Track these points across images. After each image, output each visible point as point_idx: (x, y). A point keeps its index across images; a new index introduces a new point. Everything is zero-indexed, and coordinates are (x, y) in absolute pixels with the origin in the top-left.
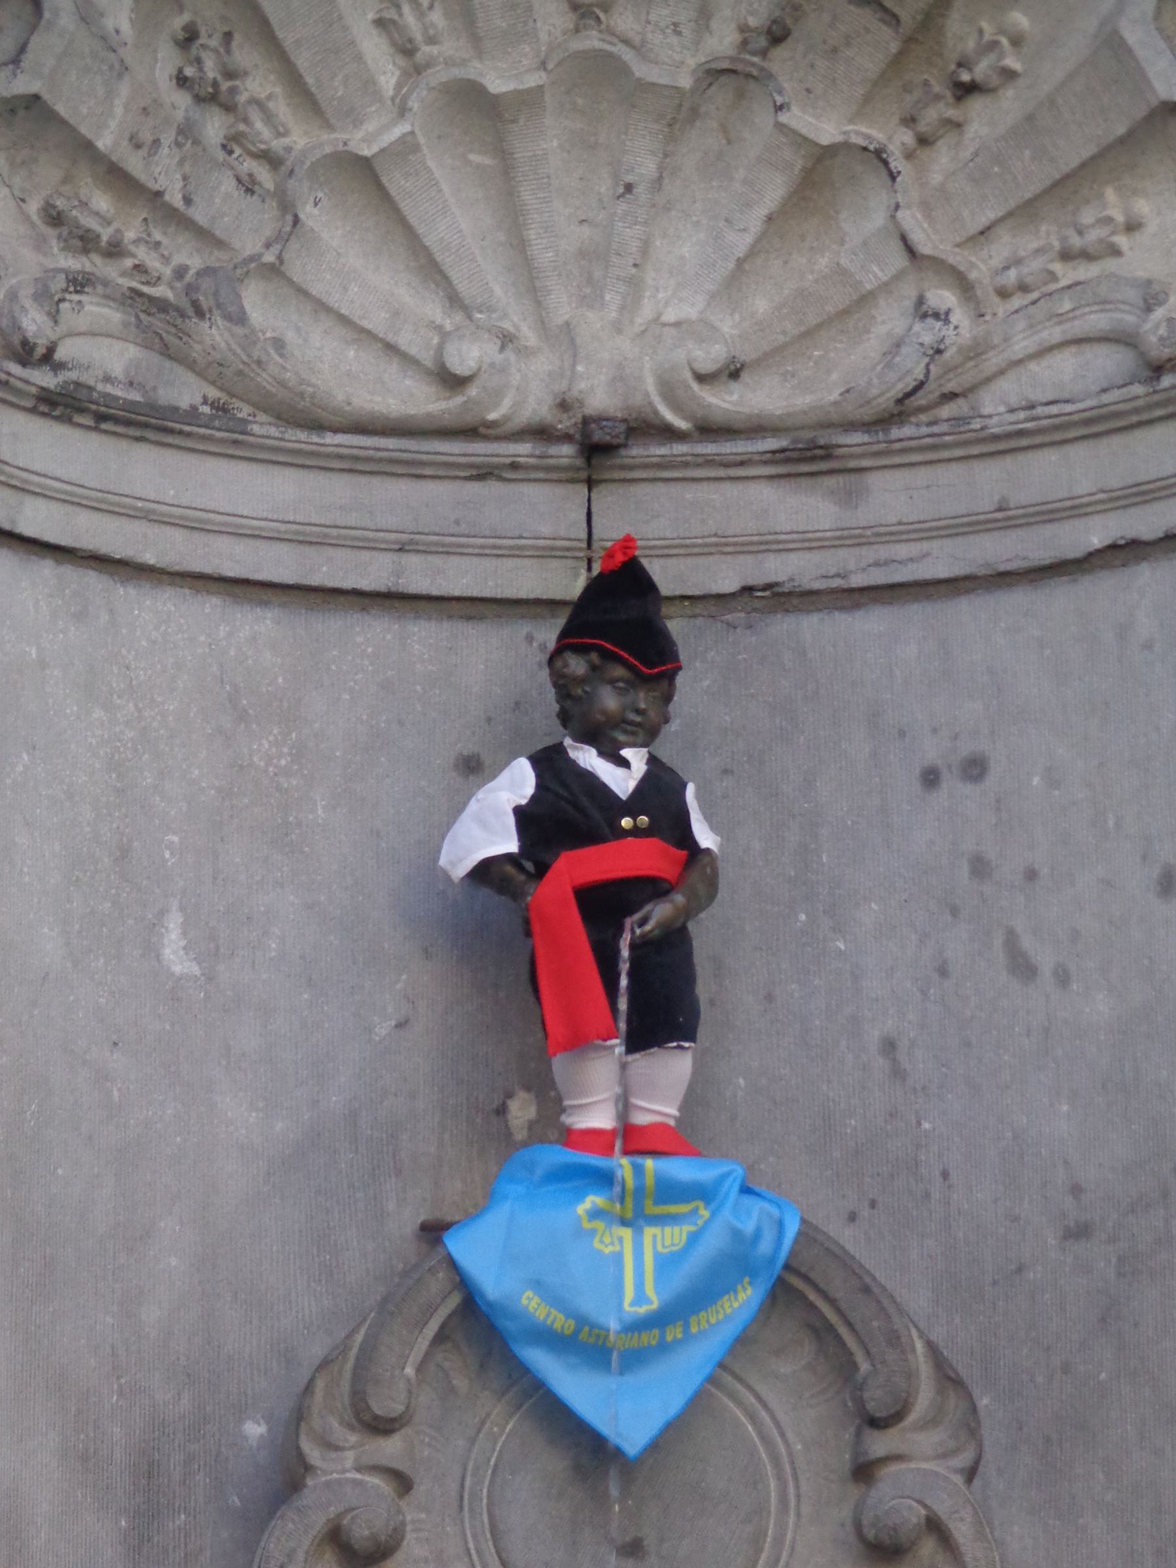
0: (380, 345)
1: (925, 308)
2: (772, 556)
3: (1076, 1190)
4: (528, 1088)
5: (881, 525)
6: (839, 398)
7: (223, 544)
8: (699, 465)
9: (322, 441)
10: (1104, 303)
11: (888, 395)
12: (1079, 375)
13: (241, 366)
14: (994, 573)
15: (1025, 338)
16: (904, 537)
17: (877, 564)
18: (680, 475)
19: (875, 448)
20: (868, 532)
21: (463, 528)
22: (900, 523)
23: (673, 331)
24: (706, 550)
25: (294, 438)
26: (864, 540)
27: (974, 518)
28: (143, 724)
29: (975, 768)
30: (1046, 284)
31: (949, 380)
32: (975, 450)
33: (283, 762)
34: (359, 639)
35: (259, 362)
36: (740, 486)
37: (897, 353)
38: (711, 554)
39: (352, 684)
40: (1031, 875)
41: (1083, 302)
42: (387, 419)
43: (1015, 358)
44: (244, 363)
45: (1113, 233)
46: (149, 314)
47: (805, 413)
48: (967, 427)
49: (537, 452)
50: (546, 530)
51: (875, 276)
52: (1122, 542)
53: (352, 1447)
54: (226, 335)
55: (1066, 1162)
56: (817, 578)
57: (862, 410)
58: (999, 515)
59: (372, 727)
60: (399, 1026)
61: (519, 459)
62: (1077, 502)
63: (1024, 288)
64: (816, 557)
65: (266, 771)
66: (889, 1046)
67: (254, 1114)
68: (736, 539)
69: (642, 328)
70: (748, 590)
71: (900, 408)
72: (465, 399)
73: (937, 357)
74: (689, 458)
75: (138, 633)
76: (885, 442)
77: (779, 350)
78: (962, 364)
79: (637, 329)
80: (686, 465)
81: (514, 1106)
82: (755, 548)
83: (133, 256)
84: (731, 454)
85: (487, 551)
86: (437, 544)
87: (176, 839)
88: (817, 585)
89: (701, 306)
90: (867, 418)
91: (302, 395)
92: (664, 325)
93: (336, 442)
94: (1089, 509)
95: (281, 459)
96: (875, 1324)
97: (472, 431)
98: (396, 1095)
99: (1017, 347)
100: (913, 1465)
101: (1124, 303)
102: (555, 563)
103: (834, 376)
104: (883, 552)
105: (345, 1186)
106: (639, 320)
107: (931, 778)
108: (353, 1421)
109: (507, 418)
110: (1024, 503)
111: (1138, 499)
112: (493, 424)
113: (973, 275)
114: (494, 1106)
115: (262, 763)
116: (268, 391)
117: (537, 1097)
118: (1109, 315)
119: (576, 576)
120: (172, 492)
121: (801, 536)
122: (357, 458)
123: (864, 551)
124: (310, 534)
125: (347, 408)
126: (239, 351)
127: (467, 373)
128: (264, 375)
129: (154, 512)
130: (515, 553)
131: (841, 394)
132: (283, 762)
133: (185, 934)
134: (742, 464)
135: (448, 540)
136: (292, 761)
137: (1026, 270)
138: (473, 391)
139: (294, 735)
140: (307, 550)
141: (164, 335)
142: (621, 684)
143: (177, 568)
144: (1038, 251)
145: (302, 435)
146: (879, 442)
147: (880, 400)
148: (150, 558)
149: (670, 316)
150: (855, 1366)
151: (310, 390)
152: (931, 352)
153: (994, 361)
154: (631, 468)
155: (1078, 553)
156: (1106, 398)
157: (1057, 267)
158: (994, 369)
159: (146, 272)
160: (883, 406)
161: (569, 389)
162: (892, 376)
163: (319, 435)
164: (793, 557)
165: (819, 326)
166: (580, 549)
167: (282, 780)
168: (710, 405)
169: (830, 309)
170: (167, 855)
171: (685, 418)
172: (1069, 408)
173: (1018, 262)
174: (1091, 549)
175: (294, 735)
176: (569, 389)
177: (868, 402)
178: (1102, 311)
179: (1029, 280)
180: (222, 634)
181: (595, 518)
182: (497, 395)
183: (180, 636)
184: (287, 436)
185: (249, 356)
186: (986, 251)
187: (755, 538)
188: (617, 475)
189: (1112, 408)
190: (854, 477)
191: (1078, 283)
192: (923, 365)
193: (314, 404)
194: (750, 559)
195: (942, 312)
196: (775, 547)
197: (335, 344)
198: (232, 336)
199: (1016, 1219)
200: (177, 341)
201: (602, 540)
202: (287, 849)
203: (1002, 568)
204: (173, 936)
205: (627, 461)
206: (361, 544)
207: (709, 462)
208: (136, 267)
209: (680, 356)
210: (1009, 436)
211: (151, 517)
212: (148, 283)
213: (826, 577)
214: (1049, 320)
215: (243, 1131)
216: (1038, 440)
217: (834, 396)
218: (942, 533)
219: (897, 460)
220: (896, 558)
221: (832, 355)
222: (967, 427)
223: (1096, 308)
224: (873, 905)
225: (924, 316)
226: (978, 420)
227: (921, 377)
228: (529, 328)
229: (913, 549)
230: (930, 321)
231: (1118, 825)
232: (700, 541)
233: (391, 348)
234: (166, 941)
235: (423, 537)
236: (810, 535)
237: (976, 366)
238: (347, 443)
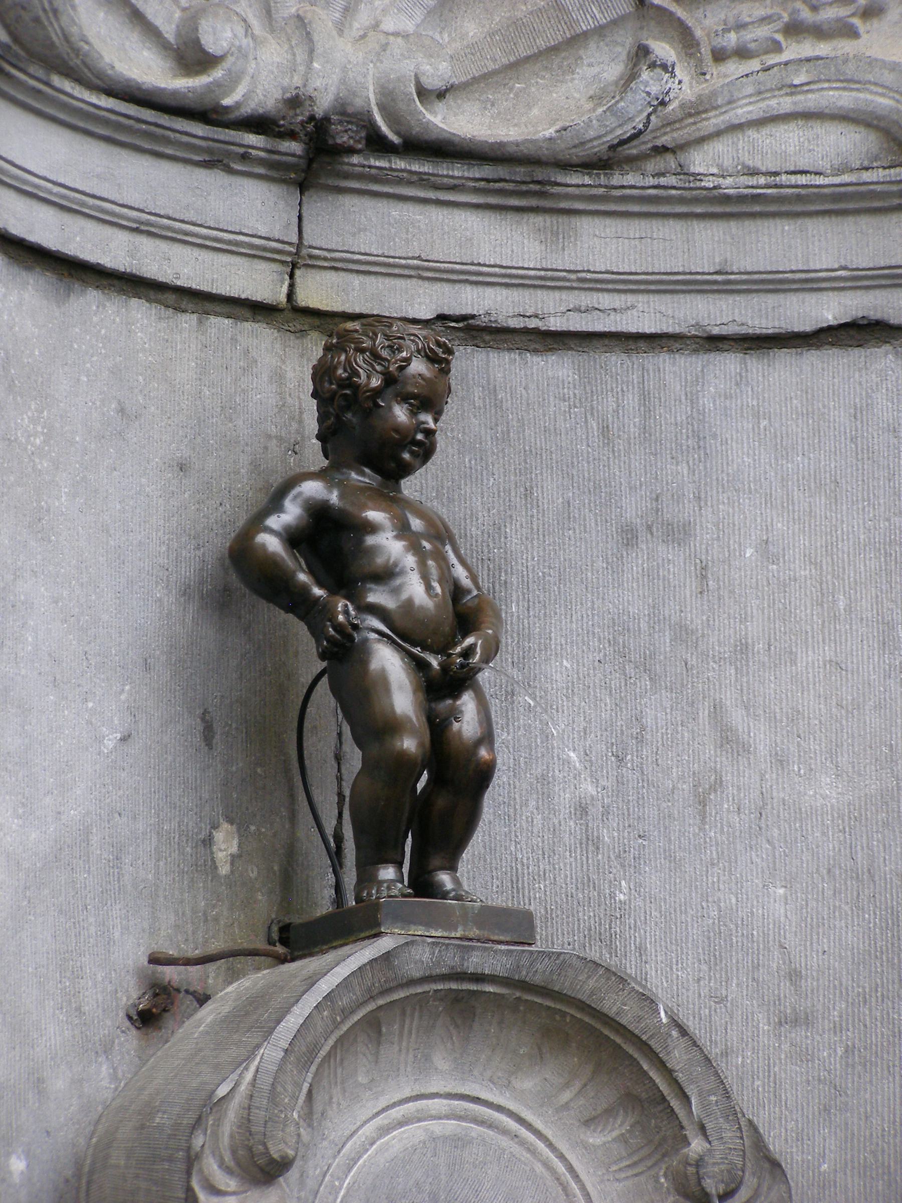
0: (128, 10)
1: (652, 57)
2: (469, 288)
3: (794, 976)
4: (231, 821)
5: (589, 271)
6: (554, 135)
8: (410, 183)
10: (849, 82)
11: (605, 139)
12: (825, 151)
13: (41, 13)
14: (705, 335)
15: (750, 103)
16: (610, 286)
17: (578, 310)
18: (391, 191)
19: (595, 191)
20: (573, 276)
21: (190, 216)
22: (607, 272)
23: (400, 40)
24: (406, 272)
25: (79, 96)
26: (568, 284)
27: (688, 277)
29: (678, 533)
30: (767, 52)
31: (665, 134)
32: (699, 210)
33: (38, 441)
34: (95, 319)
37: (622, 99)
38: (410, 277)
40: (743, 648)
41: (823, 77)
42: (139, 89)
43: (737, 122)
44: (44, 10)
45: (853, 15)
47: (517, 145)
48: (698, 184)
49: (269, 147)
51: (594, 17)
52: (865, 322)
53: (234, 1193)
55: (782, 947)
56: (514, 316)
57: (574, 150)
58: (719, 278)
59: (104, 414)
60: (124, 739)
61: (250, 151)
62: (813, 275)
63: (742, 53)
64: (515, 295)
65: (26, 449)
66: (582, 809)
67: (16, 821)
68: (438, 265)
69: (361, 33)
70: (442, 317)
71: (611, 154)
72: (211, 79)
73: (659, 108)
74: (405, 175)
76: (606, 187)
77: (485, 77)
78: (682, 119)
79: (355, 33)
80: (400, 181)
81: (219, 836)
82: (455, 277)
84: (447, 176)
85: (208, 243)
86: (169, 228)
88: (514, 323)
89: (419, 20)
90: (575, 160)
91: (77, 51)
92: (387, 34)
93: (109, 106)
94: (824, 285)
95: (62, 116)
96: (713, 1098)
97: (206, 113)
98: (120, 814)
99: (740, 111)
101: (876, 84)
102: (262, 265)
103: (535, 111)
105: (80, 908)
106: (356, 25)
107: (629, 537)
108: (232, 1164)
109: (238, 105)
110: (749, 269)
111: (889, 282)
112: (227, 109)
113: (698, 33)
114: (202, 836)
116: (53, 44)
117: (238, 830)
118: (854, 94)
119: (282, 282)
121: (503, 271)
122: (119, 127)
123: (564, 295)
125: (110, 72)
127: (219, 53)
128: (56, 26)
130: (230, 249)
131: (557, 131)
134: (453, 188)
135: (178, 225)
137: (748, 35)
138: (218, 73)
139: (45, 413)
140: (67, 218)
144: (765, 20)
146: (600, 186)
147: (595, 143)
149: (389, 25)
150: (686, 1142)
152: (656, 103)
153: (715, 121)
154: (347, 176)
155: (808, 328)
156: (866, 176)
157: (779, 37)
158: (712, 129)
160: (596, 150)
161: (305, 86)
162: (611, 122)
163: (98, 97)
164: (489, 291)
165: (527, 59)
166: (289, 254)
167: (37, 460)
168: (429, 122)
169: (542, 43)
171: (398, 133)
172: (820, 180)
173: (740, 26)
174: (825, 325)
176: (305, 86)
177: (583, 144)
178: (844, 89)
179: (752, 46)
181: (305, 222)
182: (234, 79)
186: (701, 10)
187: (458, 267)
188: (331, 182)
189: (872, 187)
190: (563, 219)
191: (818, 58)
192: (645, 114)
193: (84, 62)
194: (447, 288)
195: (669, 64)
196: (474, 278)
199: (722, 1000)
201: (311, 247)
202: (40, 535)
203: (716, 331)
205: (346, 168)
207: (422, 180)
209: (407, 68)
210: (741, 199)
213: (524, 316)
214: (780, 89)
216: (773, 208)
217: (550, 132)
218: (653, 287)
219: (613, 207)
220: (596, 306)
221: (533, 89)
222: (698, 184)
223: (838, 85)
224: (565, 663)
225: (652, 66)
226: (711, 178)
227: (641, 126)
228: (255, 16)
229: (617, 300)
230: (658, 70)
231: (849, 609)
232: (403, 262)
235: (159, 219)
236: (514, 271)
237: (695, 123)
238: (117, 109)
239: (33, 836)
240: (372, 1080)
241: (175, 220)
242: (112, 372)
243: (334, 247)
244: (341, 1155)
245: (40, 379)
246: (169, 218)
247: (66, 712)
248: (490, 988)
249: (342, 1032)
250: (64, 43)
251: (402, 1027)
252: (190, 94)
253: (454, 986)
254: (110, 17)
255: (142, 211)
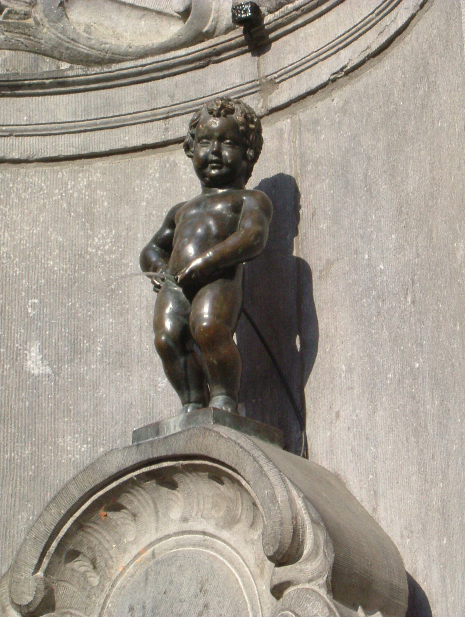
0: (154, 13)
2: (342, 51)
7: (62, 140)
8: (300, 16)
9: (110, 70)
20: (374, 15)
28: (15, 243)
33: (107, 247)
35: (73, 40)
36: (323, 18)
38: (316, 63)
39: (146, 196)
42: (152, 49)
46: (10, 32)
50: (238, 82)
54: (53, 30)
65: (97, 254)
67: (85, 446)
75: (13, 195)
83: (6, 7)
87: (36, 301)
93: (117, 68)
100: (300, 586)
104: (383, 23)
115: (94, 251)
120: (25, 118)
124: (115, 122)
125: (130, 50)
126: (62, 37)
129: (16, 131)
132: (107, 247)
133: (41, 351)
135: (190, 103)
136: (112, 246)
139: (114, 231)
141: (22, 40)
142: (205, 141)
143: (35, 157)
145: (97, 69)
148: (15, 155)
151: (107, 46)
159: (16, 13)
170: (30, 311)
175: (114, 231)
180: (69, 187)
183: (42, 192)
184: (88, 73)
185: (68, 38)
193: (113, 53)
197: (134, 21)
198: (56, 29)
200: (30, 42)
204: (33, 354)
206: (144, 120)
208: (10, 12)
211: (15, 134)
212: (20, 18)
215: (78, 457)
233: (159, 13)
234: (28, 357)
239: (102, 449)
240: (136, 537)
241: (188, 102)
242: (165, 193)
243: (277, 70)
244: (116, 587)
245: (109, 216)
246: (184, 102)
247: (131, 378)
248: (165, 464)
249: (75, 518)
250: (93, 51)
251: (139, 501)
252: (181, 37)
253: (145, 470)
254: (148, 22)
255: (166, 107)
